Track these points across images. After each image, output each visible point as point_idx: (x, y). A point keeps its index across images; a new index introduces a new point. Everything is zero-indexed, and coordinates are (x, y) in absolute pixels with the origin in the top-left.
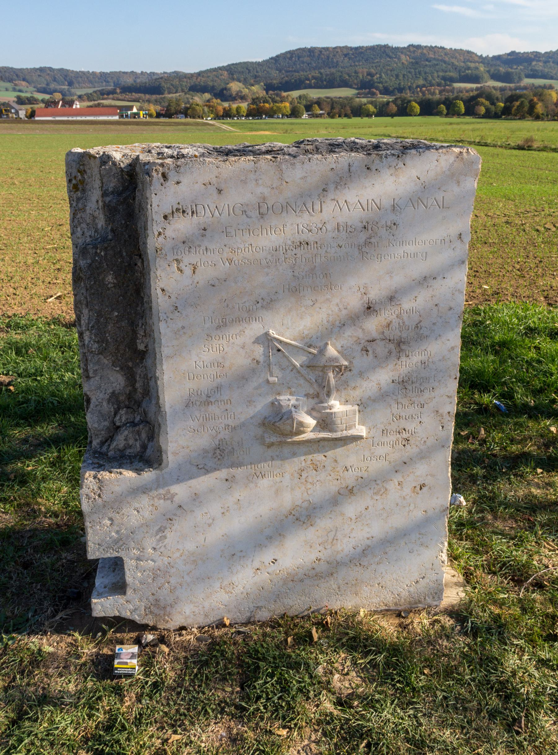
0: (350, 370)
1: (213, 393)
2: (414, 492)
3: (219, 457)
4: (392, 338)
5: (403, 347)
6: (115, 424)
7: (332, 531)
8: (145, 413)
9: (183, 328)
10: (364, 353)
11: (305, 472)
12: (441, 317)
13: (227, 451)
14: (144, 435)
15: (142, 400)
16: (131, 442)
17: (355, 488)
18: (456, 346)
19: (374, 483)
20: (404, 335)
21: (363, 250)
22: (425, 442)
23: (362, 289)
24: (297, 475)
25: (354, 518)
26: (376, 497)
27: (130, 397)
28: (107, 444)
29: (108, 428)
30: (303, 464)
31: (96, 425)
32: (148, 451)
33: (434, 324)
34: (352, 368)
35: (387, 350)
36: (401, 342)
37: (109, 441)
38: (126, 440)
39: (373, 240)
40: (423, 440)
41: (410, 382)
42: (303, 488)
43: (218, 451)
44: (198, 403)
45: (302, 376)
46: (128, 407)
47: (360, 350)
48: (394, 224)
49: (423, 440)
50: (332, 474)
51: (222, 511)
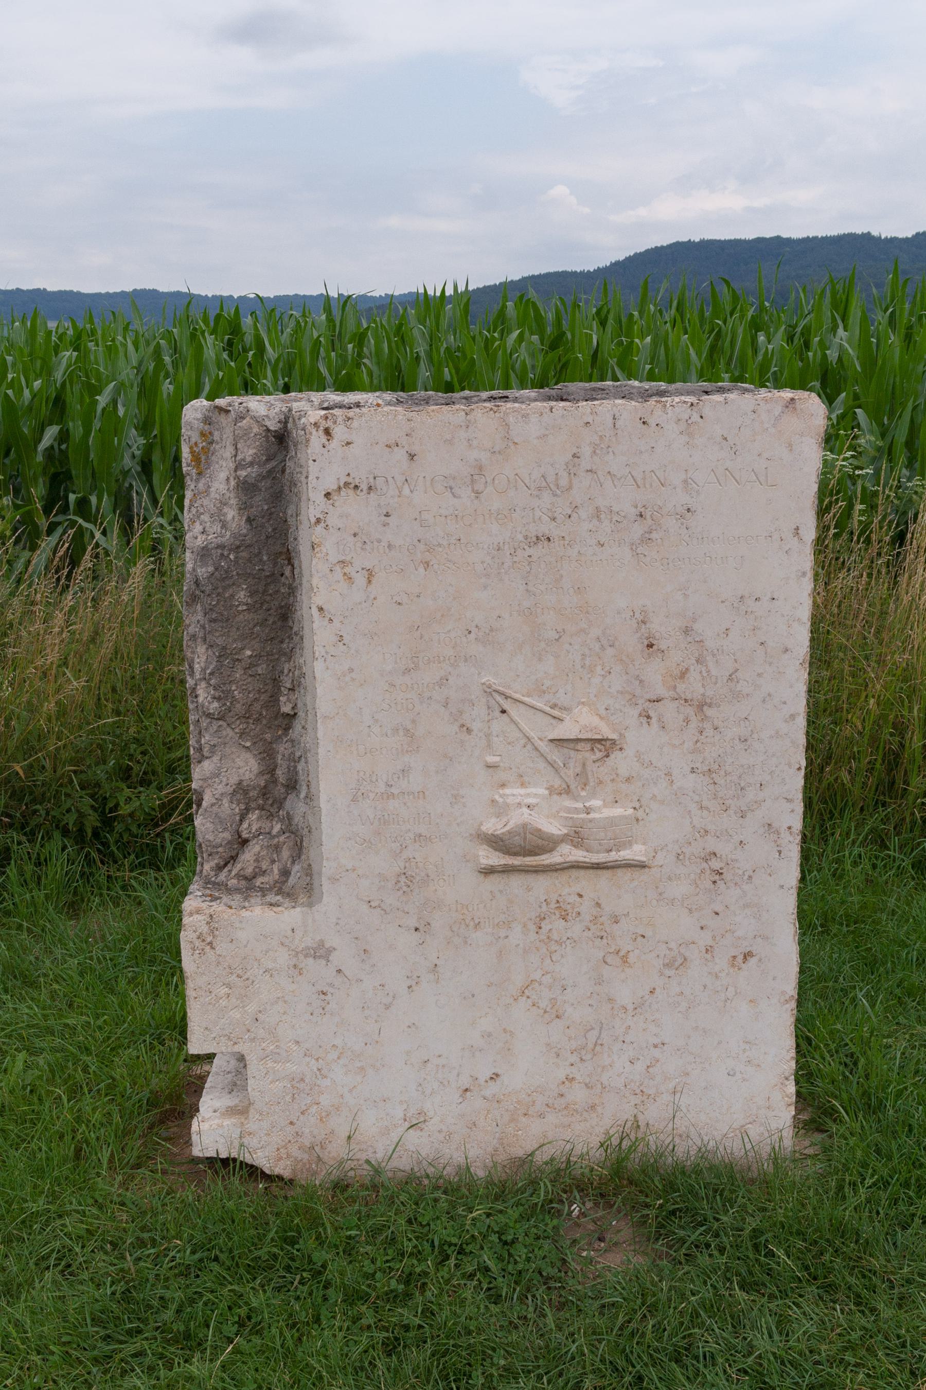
0: (621, 749)
1: (396, 779)
2: (733, 966)
3: (405, 888)
4: (689, 697)
5: (709, 712)
6: (240, 837)
7: (593, 1029)
8: (289, 817)
9: (351, 670)
10: (644, 720)
11: (547, 921)
12: (770, 664)
13: (418, 878)
14: (286, 853)
15: (285, 798)
16: (264, 865)
17: (631, 954)
18: (799, 714)
19: (664, 946)
20: (710, 693)
21: (639, 551)
22: (750, 877)
23: (637, 615)
24: (533, 928)
25: (630, 1007)
26: (668, 972)
27: (265, 792)
28: (226, 869)
29: (229, 842)
30: (544, 908)
31: (210, 837)
32: (291, 878)
33: (759, 675)
34: (625, 746)
35: (681, 717)
36: (706, 704)
37: (230, 865)
38: (257, 860)
39: (654, 535)
40: (747, 874)
41: (722, 773)
42: (544, 950)
43: (403, 879)
44: (372, 796)
45: (542, 755)
46: (261, 808)
47: (636, 715)
48: (689, 510)
49: (747, 874)
50: (593, 927)
51: (409, 983)
